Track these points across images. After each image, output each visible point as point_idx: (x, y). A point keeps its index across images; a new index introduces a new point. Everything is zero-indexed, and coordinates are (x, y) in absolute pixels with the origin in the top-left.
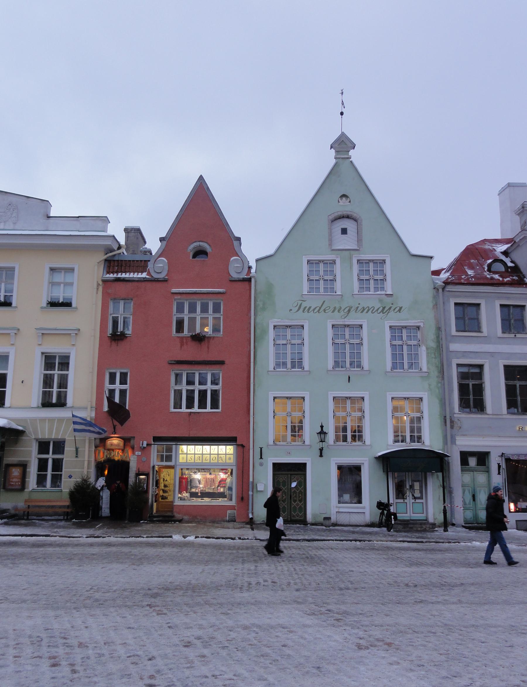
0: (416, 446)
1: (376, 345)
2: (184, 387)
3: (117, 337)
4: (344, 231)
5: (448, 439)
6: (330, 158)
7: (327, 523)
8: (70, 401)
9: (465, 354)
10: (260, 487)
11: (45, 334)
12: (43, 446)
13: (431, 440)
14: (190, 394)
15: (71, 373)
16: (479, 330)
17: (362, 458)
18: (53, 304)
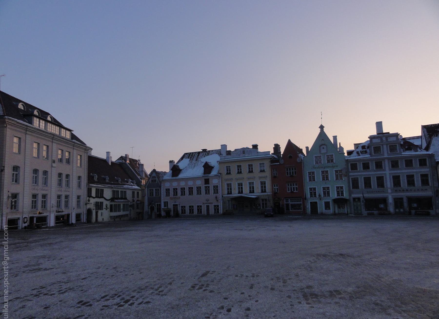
0: (342, 197)
1: (332, 175)
2: (290, 187)
3: (275, 177)
4: (323, 148)
5: (350, 195)
6: (319, 130)
7: (322, 214)
8: (267, 191)
9: (353, 176)
10: (307, 207)
11: (260, 178)
12: (263, 200)
13: (346, 195)
14: (291, 188)
15: (266, 185)
16: (357, 169)
17: (330, 200)
18: (261, 171)
